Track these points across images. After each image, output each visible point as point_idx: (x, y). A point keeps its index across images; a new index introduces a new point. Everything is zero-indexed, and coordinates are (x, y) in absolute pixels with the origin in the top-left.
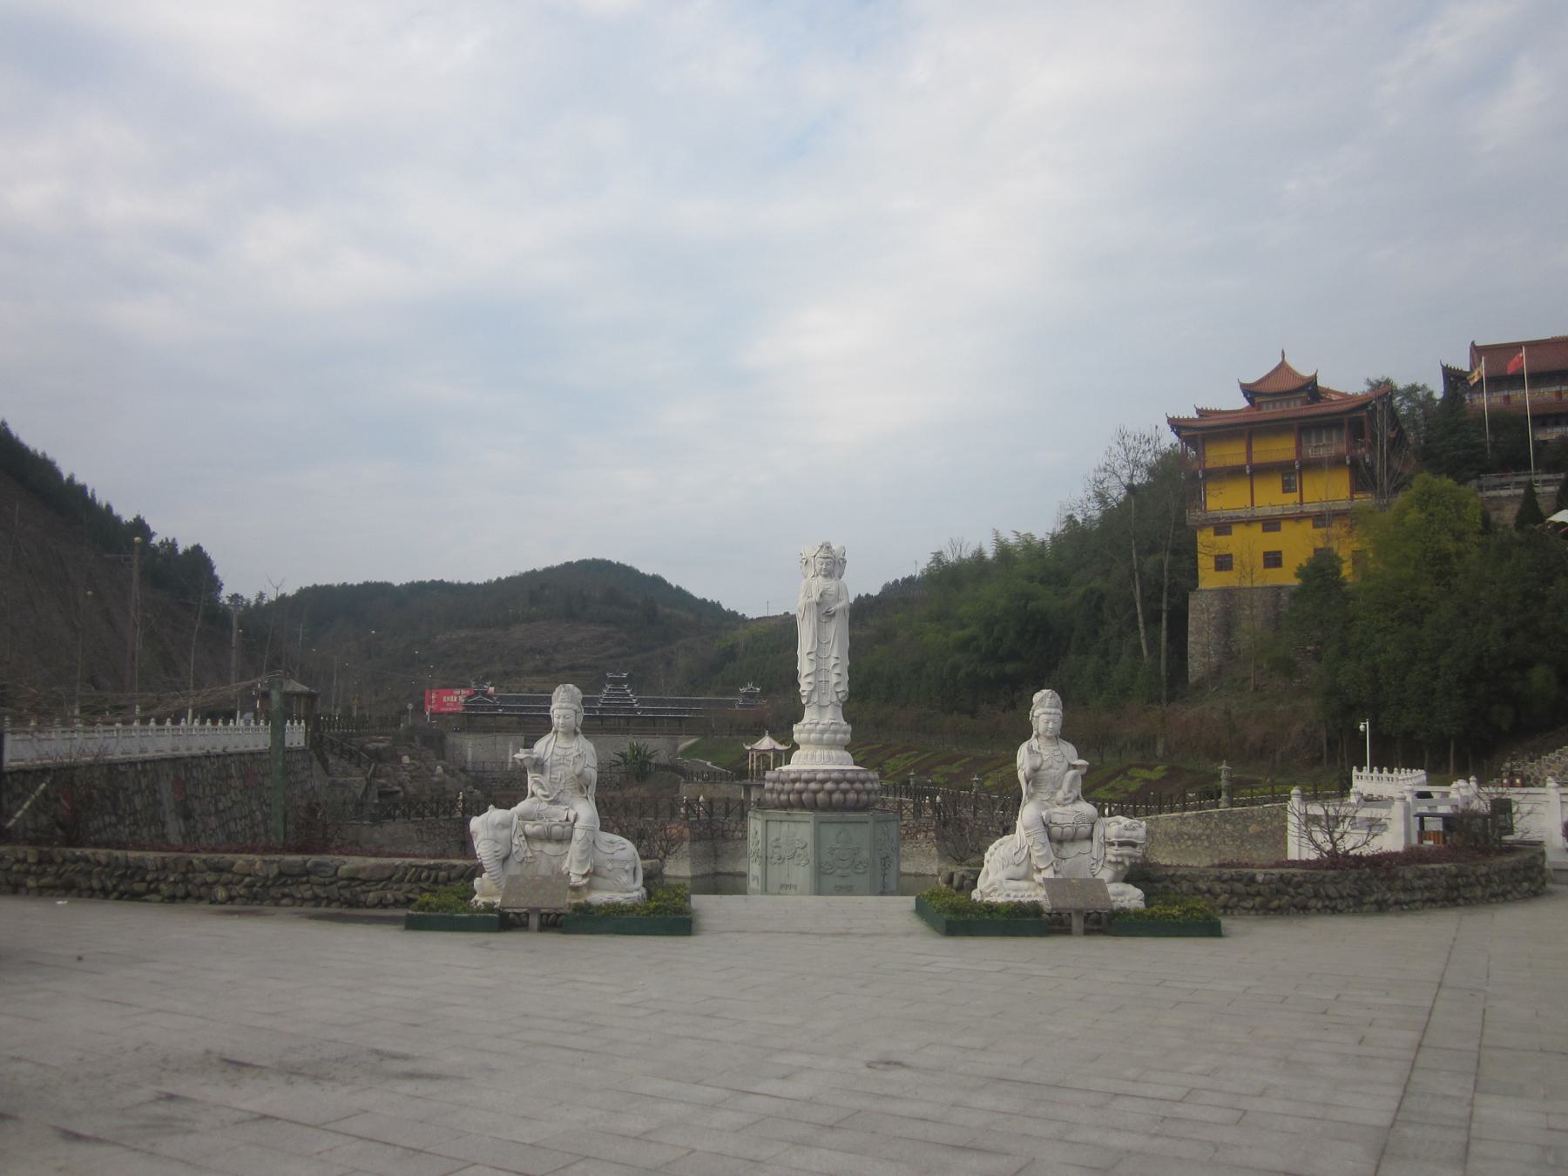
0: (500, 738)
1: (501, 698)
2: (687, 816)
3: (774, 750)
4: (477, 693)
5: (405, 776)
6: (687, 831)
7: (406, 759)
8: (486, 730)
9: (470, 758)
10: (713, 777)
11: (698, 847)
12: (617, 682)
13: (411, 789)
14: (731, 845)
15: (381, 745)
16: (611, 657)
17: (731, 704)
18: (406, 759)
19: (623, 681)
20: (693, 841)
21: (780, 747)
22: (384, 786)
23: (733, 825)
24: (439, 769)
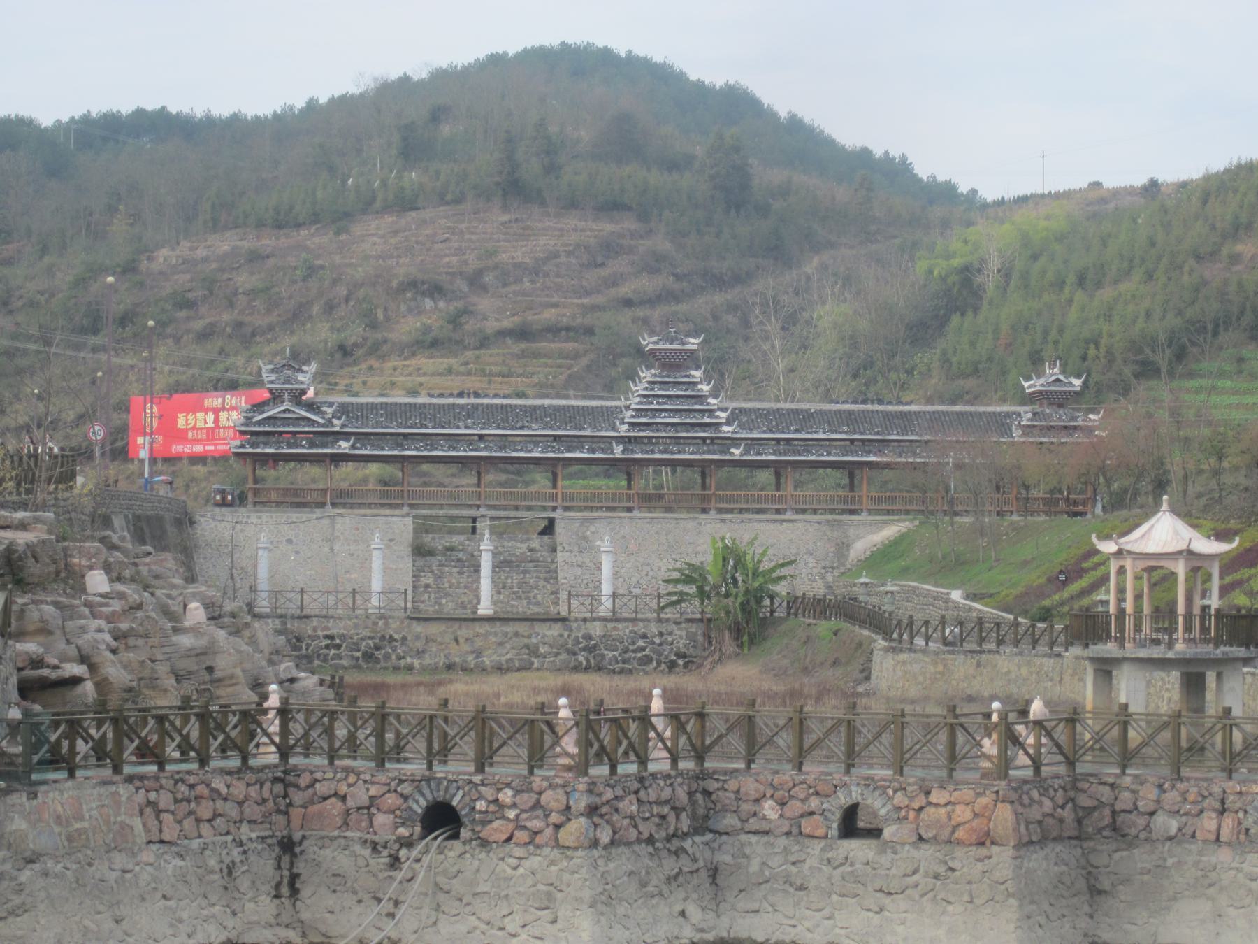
0: (345, 521)
1: (344, 410)
2: (1004, 765)
3: (1189, 553)
4: (276, 397)
5: (96, 634)
6: (1004, 815)
7: (97, 581)
8: (297, 500)
9: (263, 583)
10: (974, 636)
11: (1040, 862)
12: (673, 363)
13: (115, 672)
14: (1140, 858)
15: (21, 538)
16: (628, 303)
17: (1001, 423)
18: (97, 581)
19: (691, 359)
20: (1025, 845)
21: (1206, 546)
22: (37, 663)
23: (1153, 794)
24: (196, 613)
